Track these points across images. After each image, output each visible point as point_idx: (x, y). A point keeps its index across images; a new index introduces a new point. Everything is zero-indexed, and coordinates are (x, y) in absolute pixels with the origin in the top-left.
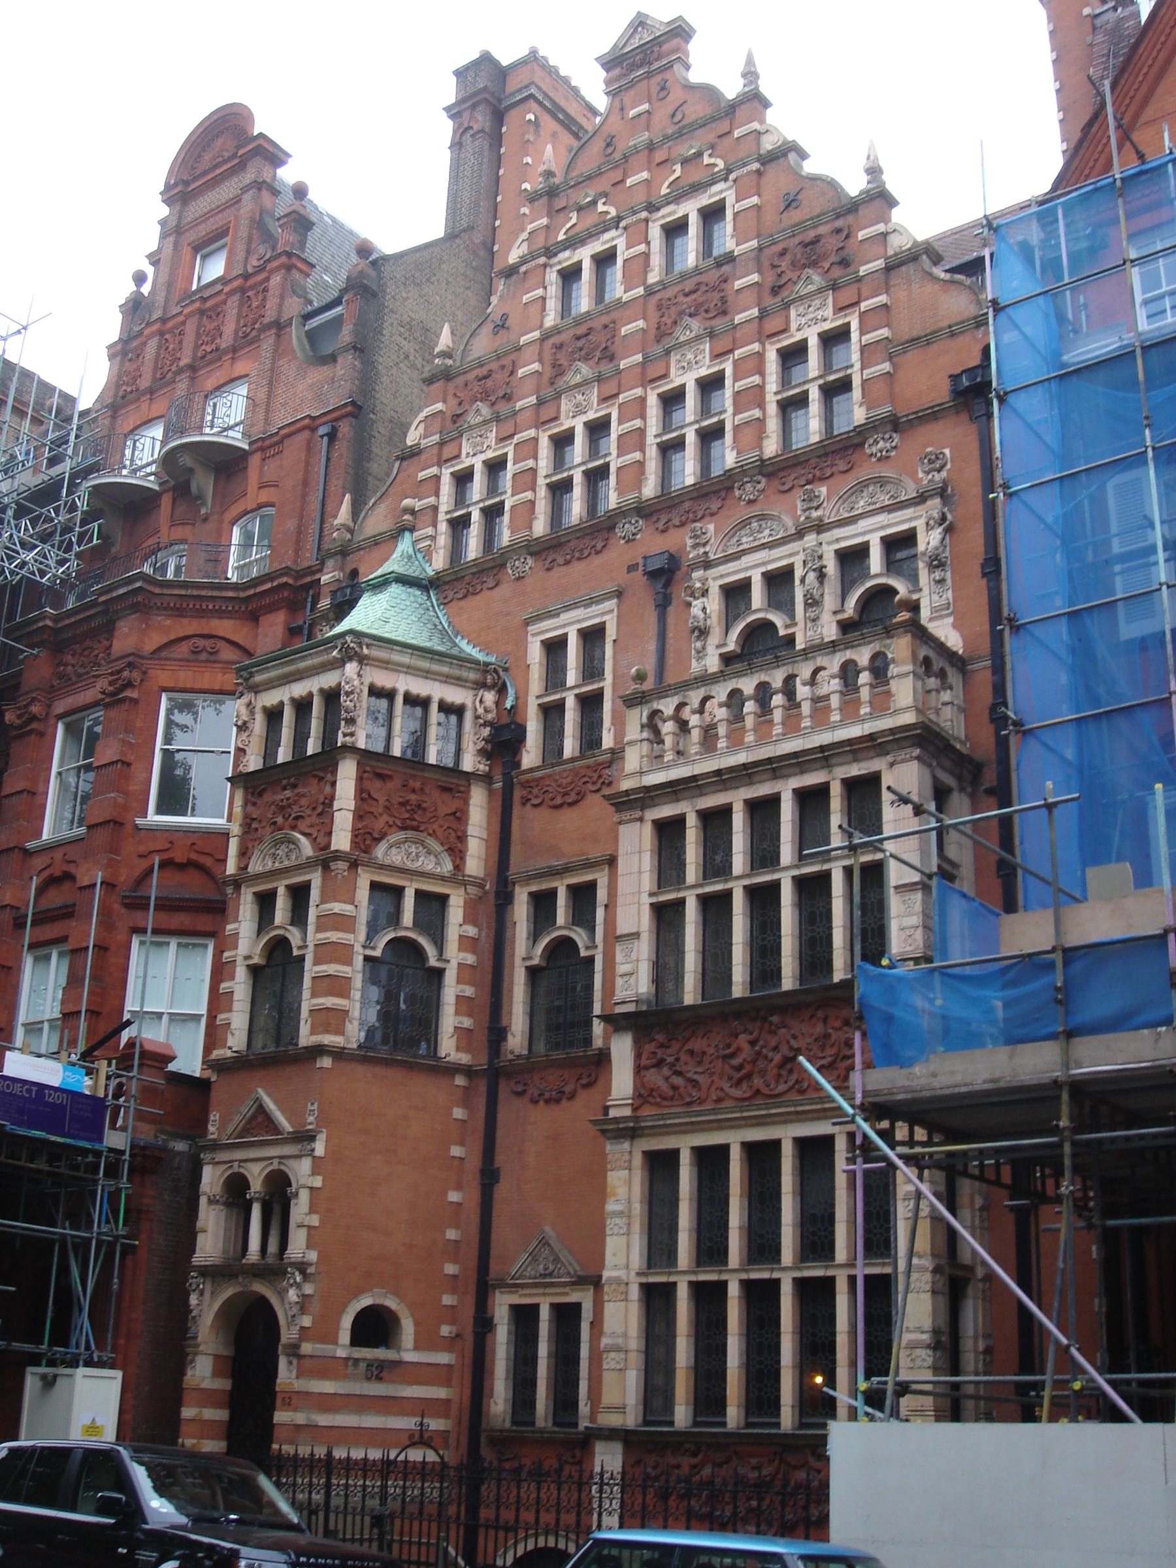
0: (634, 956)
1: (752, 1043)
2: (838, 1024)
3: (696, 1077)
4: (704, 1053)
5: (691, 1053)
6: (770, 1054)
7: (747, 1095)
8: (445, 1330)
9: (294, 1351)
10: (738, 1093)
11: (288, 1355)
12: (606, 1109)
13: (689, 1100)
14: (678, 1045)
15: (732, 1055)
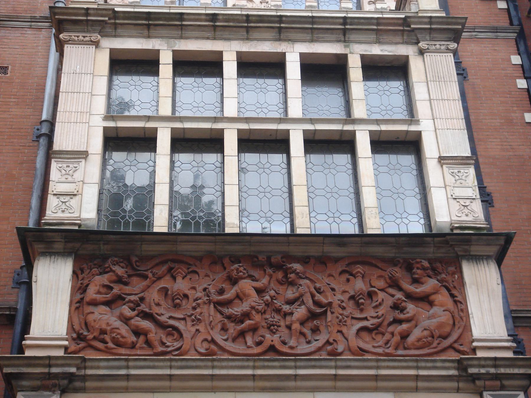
0: (78, 176)
1: (260, 291)
2: (381, 284)
3: (171, 322)
4: (186, 296)
5: (165, 291)
6: (286, 308)
7: (257, 350)
10: (237, 347)
12: (21, 350)
13: (161, 349)
14: (145, 283)
15: (228, 303)
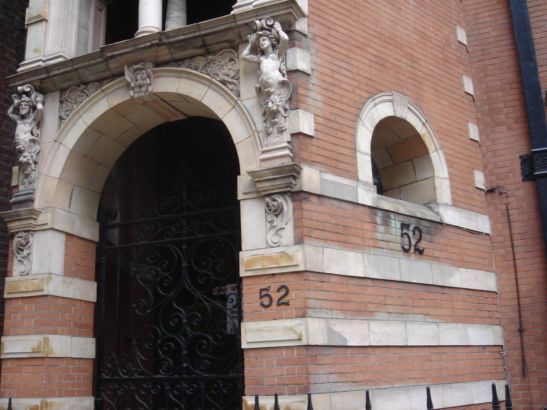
8: (480, 179)
9: (283, 185)
11: (262, 196)
